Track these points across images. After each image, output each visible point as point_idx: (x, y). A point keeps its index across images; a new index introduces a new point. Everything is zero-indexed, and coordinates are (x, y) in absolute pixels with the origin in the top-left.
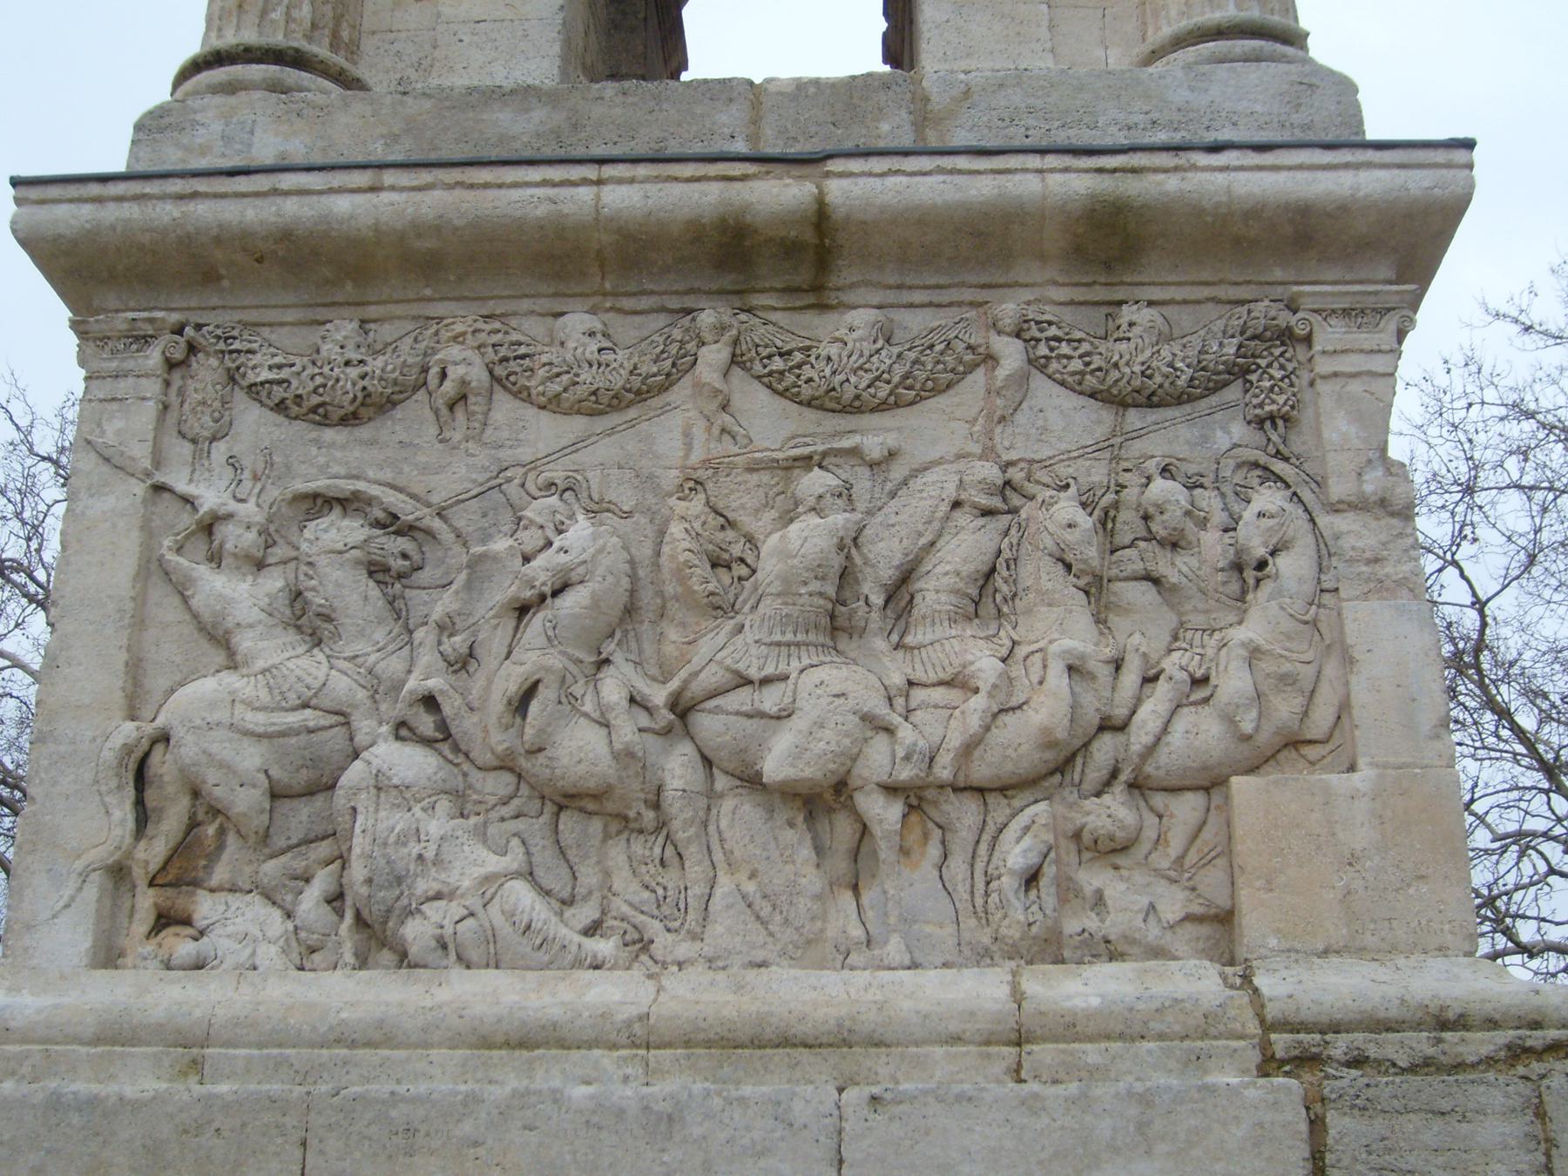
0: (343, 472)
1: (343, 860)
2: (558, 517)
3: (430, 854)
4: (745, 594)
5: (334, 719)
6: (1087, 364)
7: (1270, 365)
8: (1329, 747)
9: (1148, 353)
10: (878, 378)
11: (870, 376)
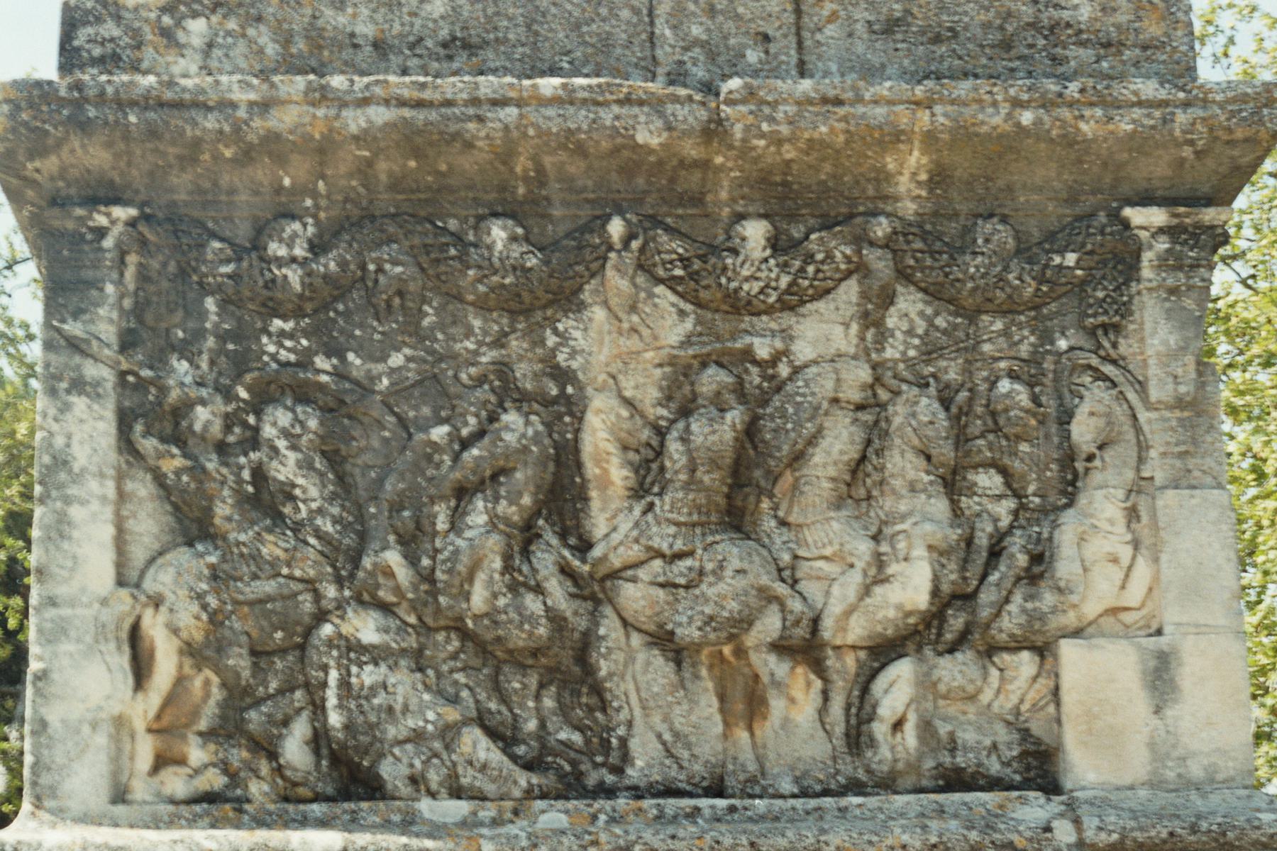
0: (292, 358)
1: (318, 708)
2: (490, 407)
3: (398, 707)
4: (653, 474)
5: (300, 586)
6: (947, 275)
7: (1104, 277)
8: (1144, 612)
9: (999, 268)
10: (767, 286)
11: (762, 284)
